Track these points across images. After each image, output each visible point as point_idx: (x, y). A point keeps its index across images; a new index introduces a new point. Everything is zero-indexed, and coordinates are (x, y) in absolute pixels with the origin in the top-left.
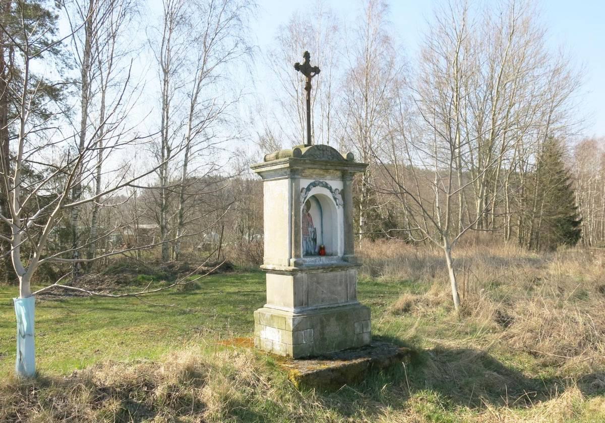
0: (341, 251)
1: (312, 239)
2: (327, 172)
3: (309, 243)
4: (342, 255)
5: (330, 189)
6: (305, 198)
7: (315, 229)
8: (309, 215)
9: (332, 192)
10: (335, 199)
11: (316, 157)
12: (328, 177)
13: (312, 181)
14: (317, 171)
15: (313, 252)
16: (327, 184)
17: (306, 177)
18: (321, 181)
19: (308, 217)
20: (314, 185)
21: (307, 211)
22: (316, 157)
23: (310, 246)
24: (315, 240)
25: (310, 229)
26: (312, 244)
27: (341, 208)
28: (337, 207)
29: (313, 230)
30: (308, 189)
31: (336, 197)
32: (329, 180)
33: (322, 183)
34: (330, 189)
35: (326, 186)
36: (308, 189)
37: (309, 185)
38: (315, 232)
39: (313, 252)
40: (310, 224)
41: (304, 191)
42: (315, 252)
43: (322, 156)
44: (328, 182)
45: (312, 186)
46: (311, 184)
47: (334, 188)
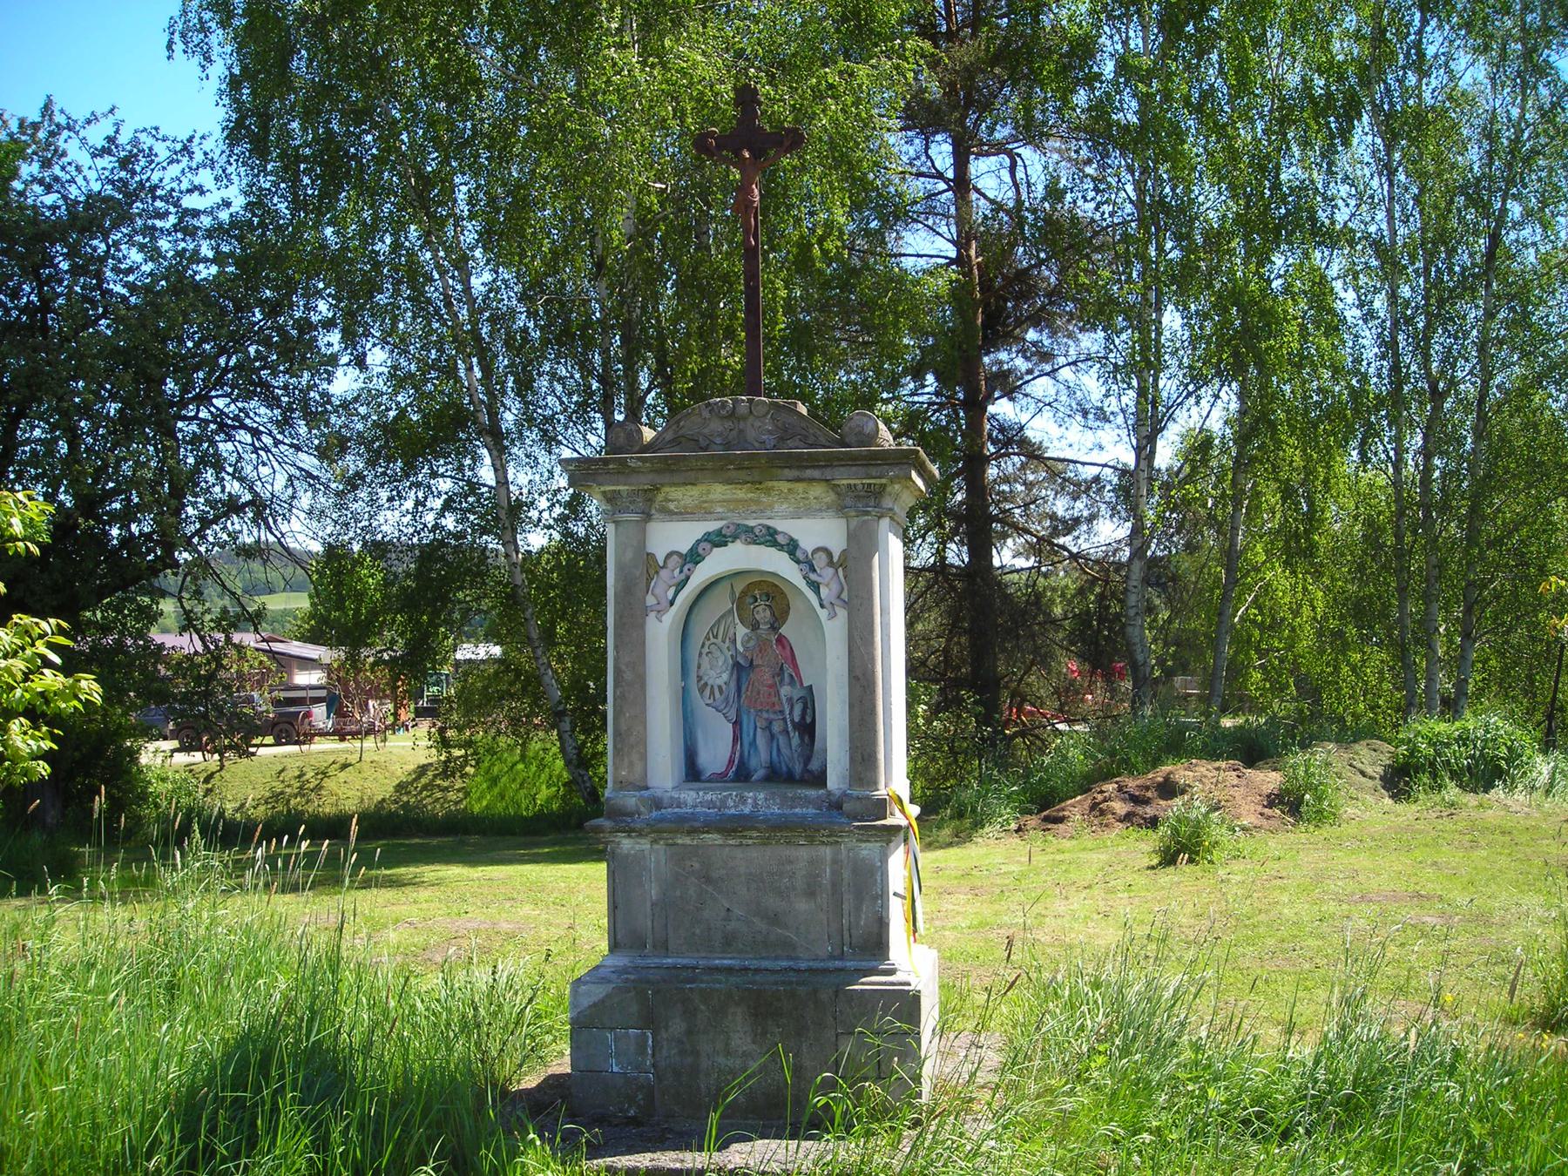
1: (796, 726)
2: (768, 491)
3: (782, 740)
5: (792, 548)
8: (781, 640)
9: (798, 562)
10: (815, 586)
12: (783, 507)
13: (713, 526)
14: (719, 491)
16: (772, 532)
17: (684, 514)
18: (752, 523)
20: (718, 540)
21: (774, 628)
23: (785, 751)
25: (785, 691)
26: (796, 740)
27: (842, 614)
28: (823, 614)
29: (797, 693)
30: (694, 557)
31: (813, 577)
33: (750, 530)
34: (792, 548)
35: (770, 538)
36: (694, 557)
37: (699, 542)
40: (788, 670)
42: (806, 770)
44: (780, 525)
45: (707, 546)
47: (807, 544)
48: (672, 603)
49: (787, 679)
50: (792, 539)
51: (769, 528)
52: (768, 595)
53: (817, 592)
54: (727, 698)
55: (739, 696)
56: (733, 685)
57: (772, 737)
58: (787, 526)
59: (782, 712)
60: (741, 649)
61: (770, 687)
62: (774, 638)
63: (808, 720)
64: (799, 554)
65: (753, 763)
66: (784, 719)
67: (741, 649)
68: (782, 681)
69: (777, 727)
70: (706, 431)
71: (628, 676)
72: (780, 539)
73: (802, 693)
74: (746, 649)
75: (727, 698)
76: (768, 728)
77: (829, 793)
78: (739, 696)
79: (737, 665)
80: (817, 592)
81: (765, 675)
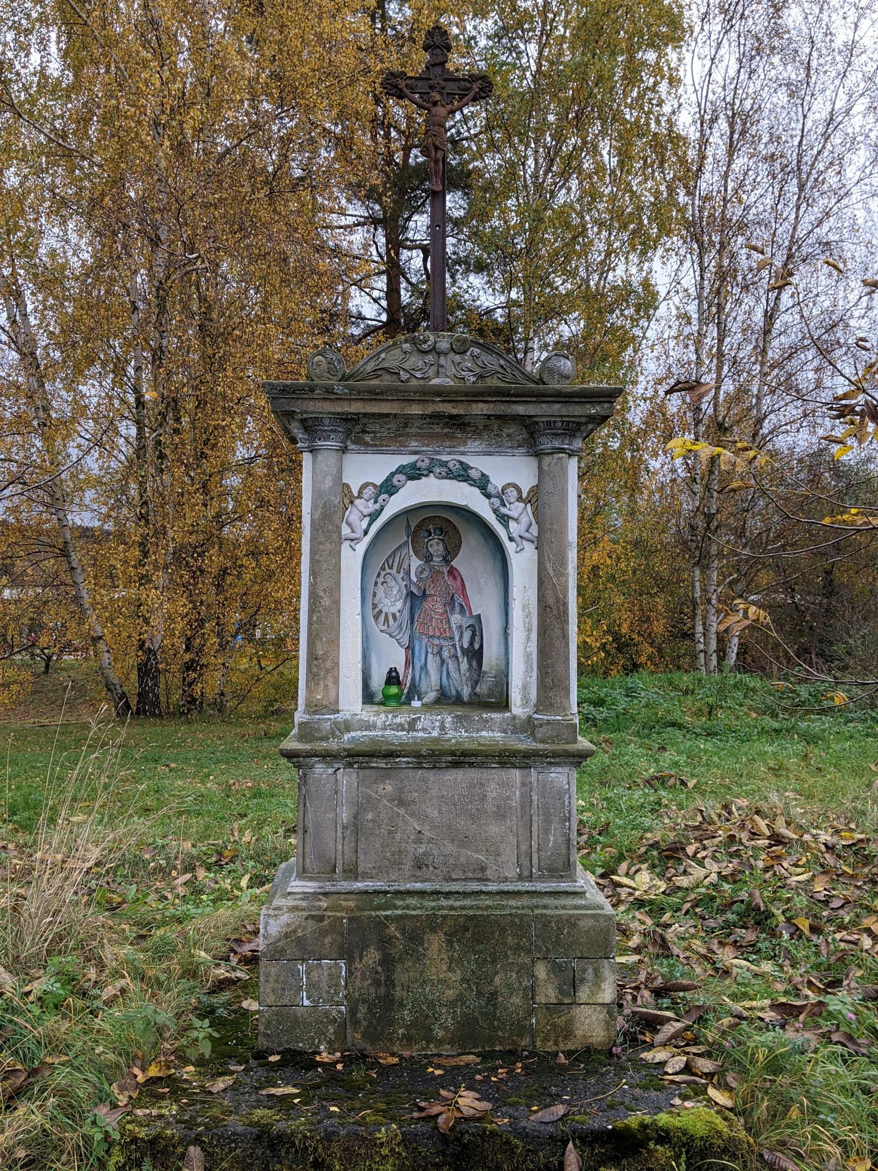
0: (525, 699)
1: (465, 652)
4: (529, 710)
5: (482, 484)
6: (374, 516)
7: (479, 616)
8: (453, 572)
9: (488, 496)
10: (504, 519)
11: (404, 376)
12: (474, 445)
13: (406, 460)
15: (466, 692)
16: (465, 467)
18: (444, 458)
19: (450, 581)
20: (413, 473)
21: (446, 560)
22: (404, 376)
23: (453, 674)
24: (475, 655)
26: (464, 666)
27: (530, 549)
29: (466, 622)
30: (389, 488)
31: (504, 510)
32: (478, 454)
33: (444, 464)
34: (482, 484)
35: (463, 474)
36: (389, 488)
37: (393, 474)
38: (476, 628)
39: (466, 692)
40: (459, 600)
41: (369, 492)
42: (474, 694)
43: (432, 371)
45: (402, 477)
46: (401, 470)
47: (497, 482)
48: (366, 533)
49: (457, 608)
50: (483, 475)
51: (461, 463)
52: (441, 530)
53: (506, 527)
54: (400, 625)
55: (412, 623)
56: (406, 612)
57: (443, 661)
58: (480, 464)
59: (452, 638)
60: (414, 579)
61: (441, 615)
62: (445, 570)
63: (477, 646)
64: (490, 489)
65: (423, 687)
66: (454, 646)
67: (414, 579)
68: (453, 609)
69: (446, 654)
70: (406, 366)
71: (326, 602)
72: (473, 473)
73: (471, 622)
74: (420, 579)
75: (400, 625)
76: (439, 653)
77: (514, 717)
78: (412, 623)
79: (410, 594)
80: (506, 527)
81: (435, 605)
